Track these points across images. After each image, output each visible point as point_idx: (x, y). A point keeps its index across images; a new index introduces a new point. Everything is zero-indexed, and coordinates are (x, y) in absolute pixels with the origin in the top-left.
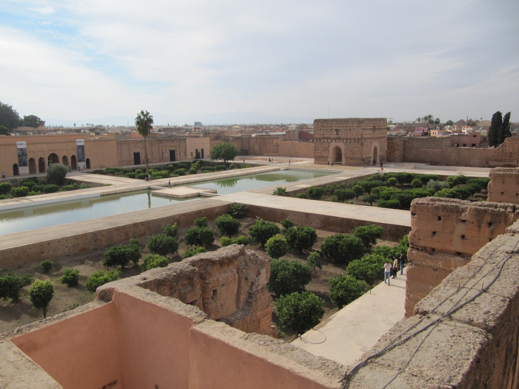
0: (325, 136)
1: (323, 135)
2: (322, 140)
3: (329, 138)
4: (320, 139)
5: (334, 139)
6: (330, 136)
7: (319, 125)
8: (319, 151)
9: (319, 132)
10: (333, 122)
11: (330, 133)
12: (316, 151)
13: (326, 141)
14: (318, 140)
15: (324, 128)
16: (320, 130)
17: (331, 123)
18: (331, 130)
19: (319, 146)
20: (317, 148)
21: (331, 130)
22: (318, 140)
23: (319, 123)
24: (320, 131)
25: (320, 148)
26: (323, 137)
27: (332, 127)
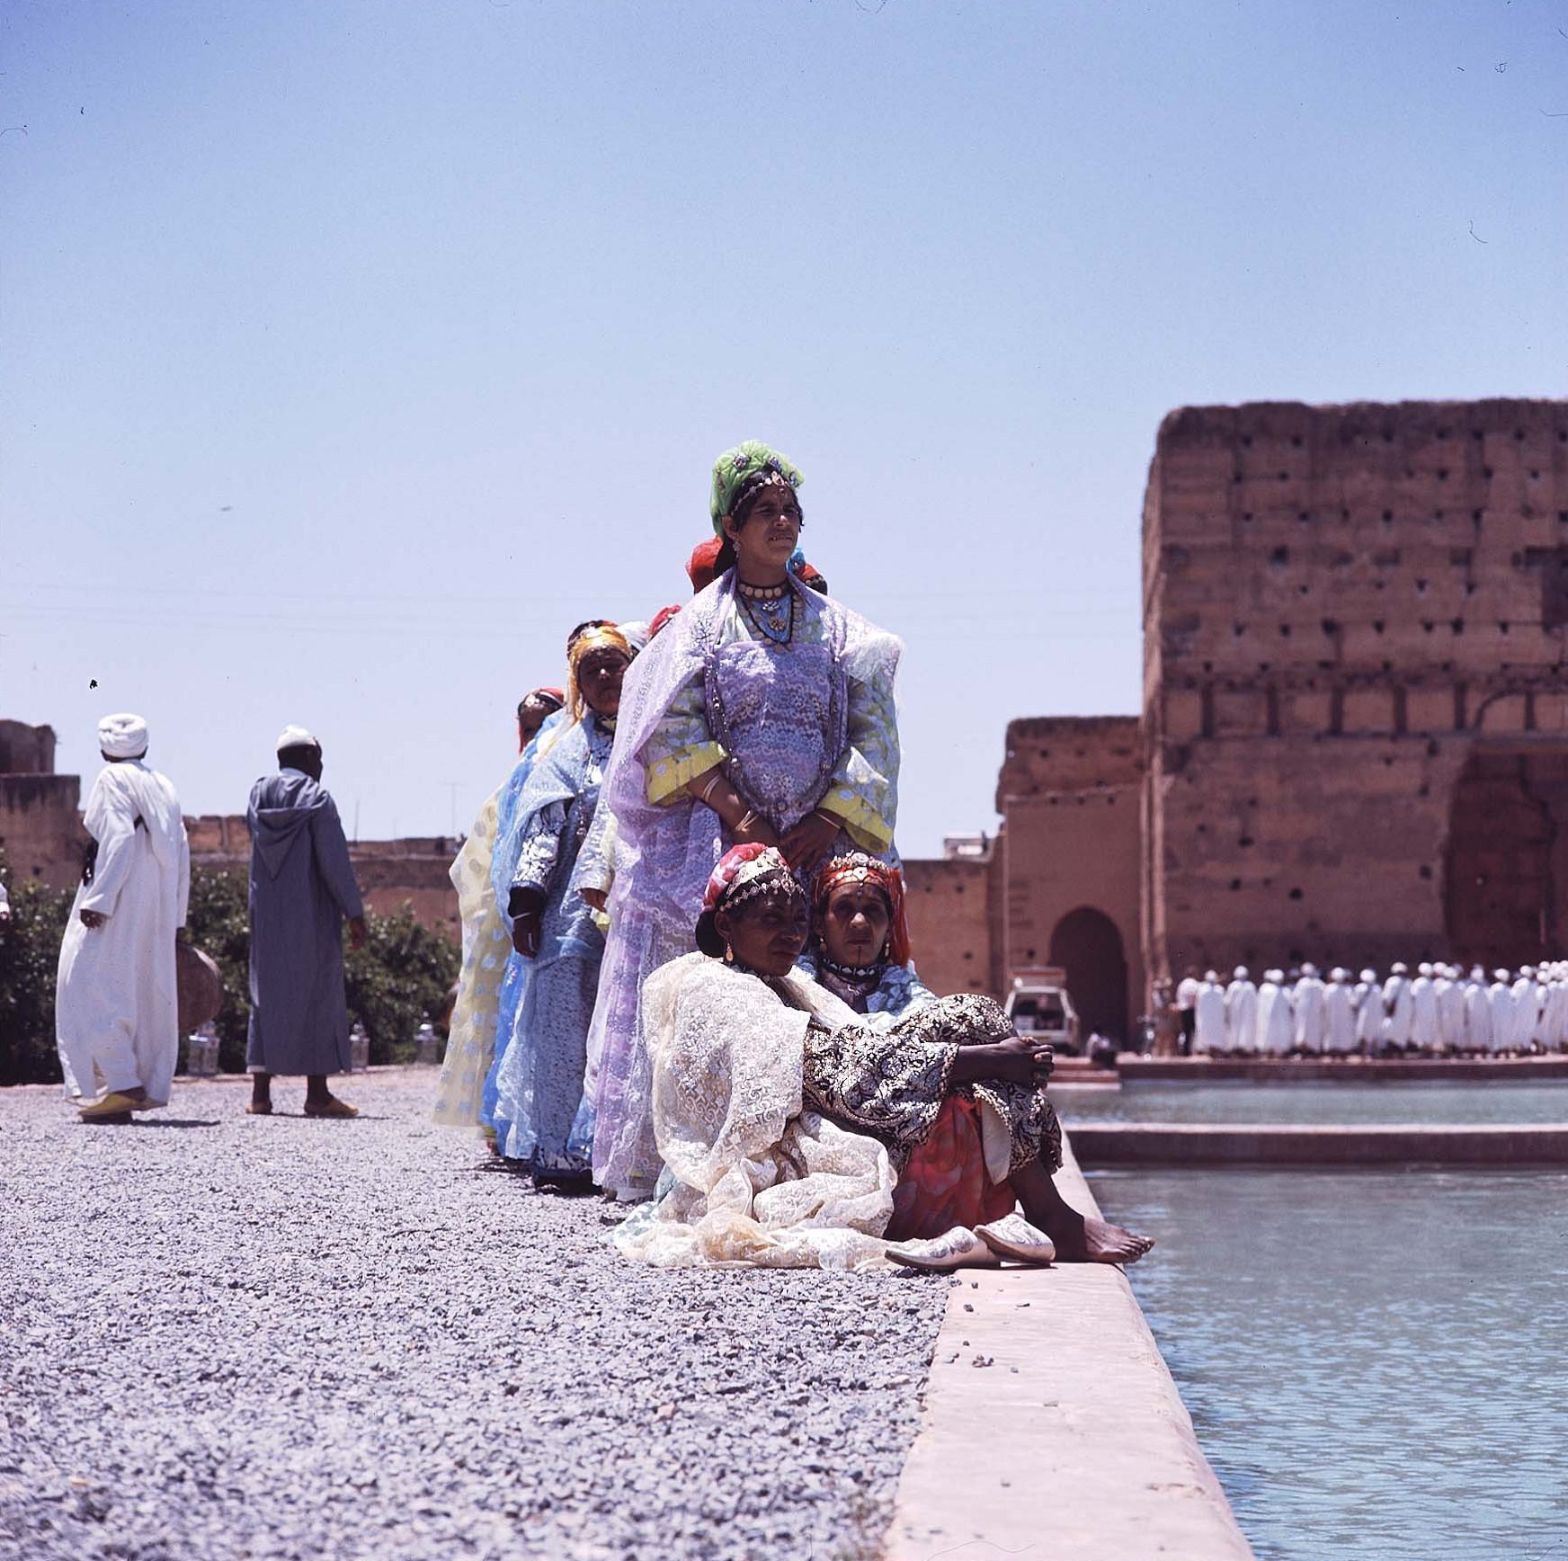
0: (1362, 645)
1: (1330, 627)
2: (1310, 708)
3: (1416, 679)
4: (1271, 692)
5: (1509, 690)
6: (1439, 643)
7: (1260, 492)
8: (1253, 868)
9: (1258, 583)
10: (1497, 448)
11: (1444, 596)
12: (1219, 871)
13: (1370, 708)
14: (1228, 704)
15: (1336, 536)
16: (1280, 555)
17: (1454, 455)
18: (1463, 558)
19: (1265, 784)
20: (1232, 825)
21: (1463, 558)
22: (1228, 704)
23: (1259, 457)
24: (1280, 576)
25: (1265, 825)
26: (1325, 665)
27: (1477, 516)
